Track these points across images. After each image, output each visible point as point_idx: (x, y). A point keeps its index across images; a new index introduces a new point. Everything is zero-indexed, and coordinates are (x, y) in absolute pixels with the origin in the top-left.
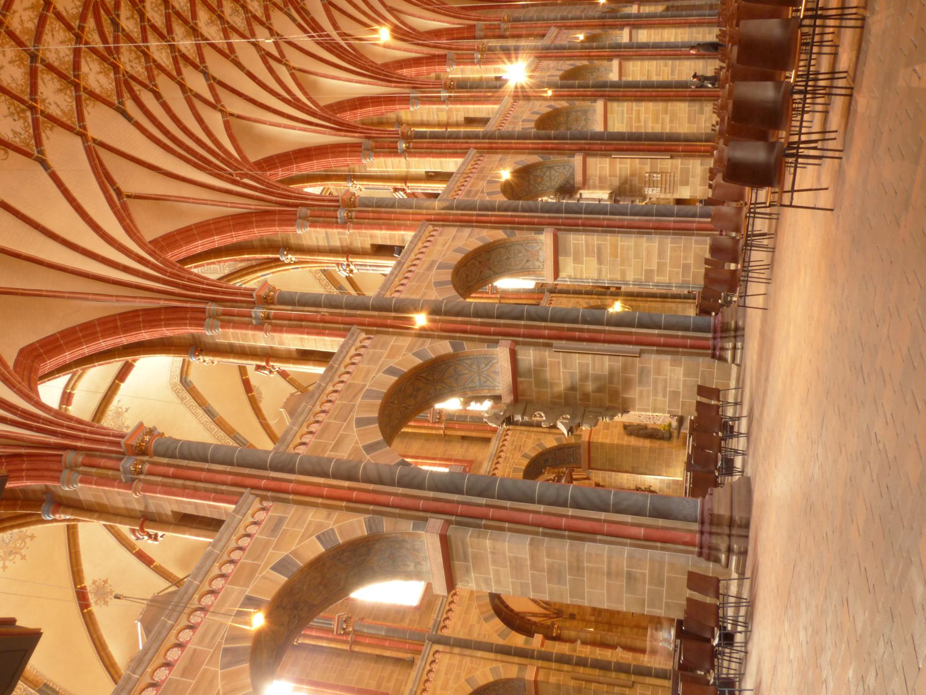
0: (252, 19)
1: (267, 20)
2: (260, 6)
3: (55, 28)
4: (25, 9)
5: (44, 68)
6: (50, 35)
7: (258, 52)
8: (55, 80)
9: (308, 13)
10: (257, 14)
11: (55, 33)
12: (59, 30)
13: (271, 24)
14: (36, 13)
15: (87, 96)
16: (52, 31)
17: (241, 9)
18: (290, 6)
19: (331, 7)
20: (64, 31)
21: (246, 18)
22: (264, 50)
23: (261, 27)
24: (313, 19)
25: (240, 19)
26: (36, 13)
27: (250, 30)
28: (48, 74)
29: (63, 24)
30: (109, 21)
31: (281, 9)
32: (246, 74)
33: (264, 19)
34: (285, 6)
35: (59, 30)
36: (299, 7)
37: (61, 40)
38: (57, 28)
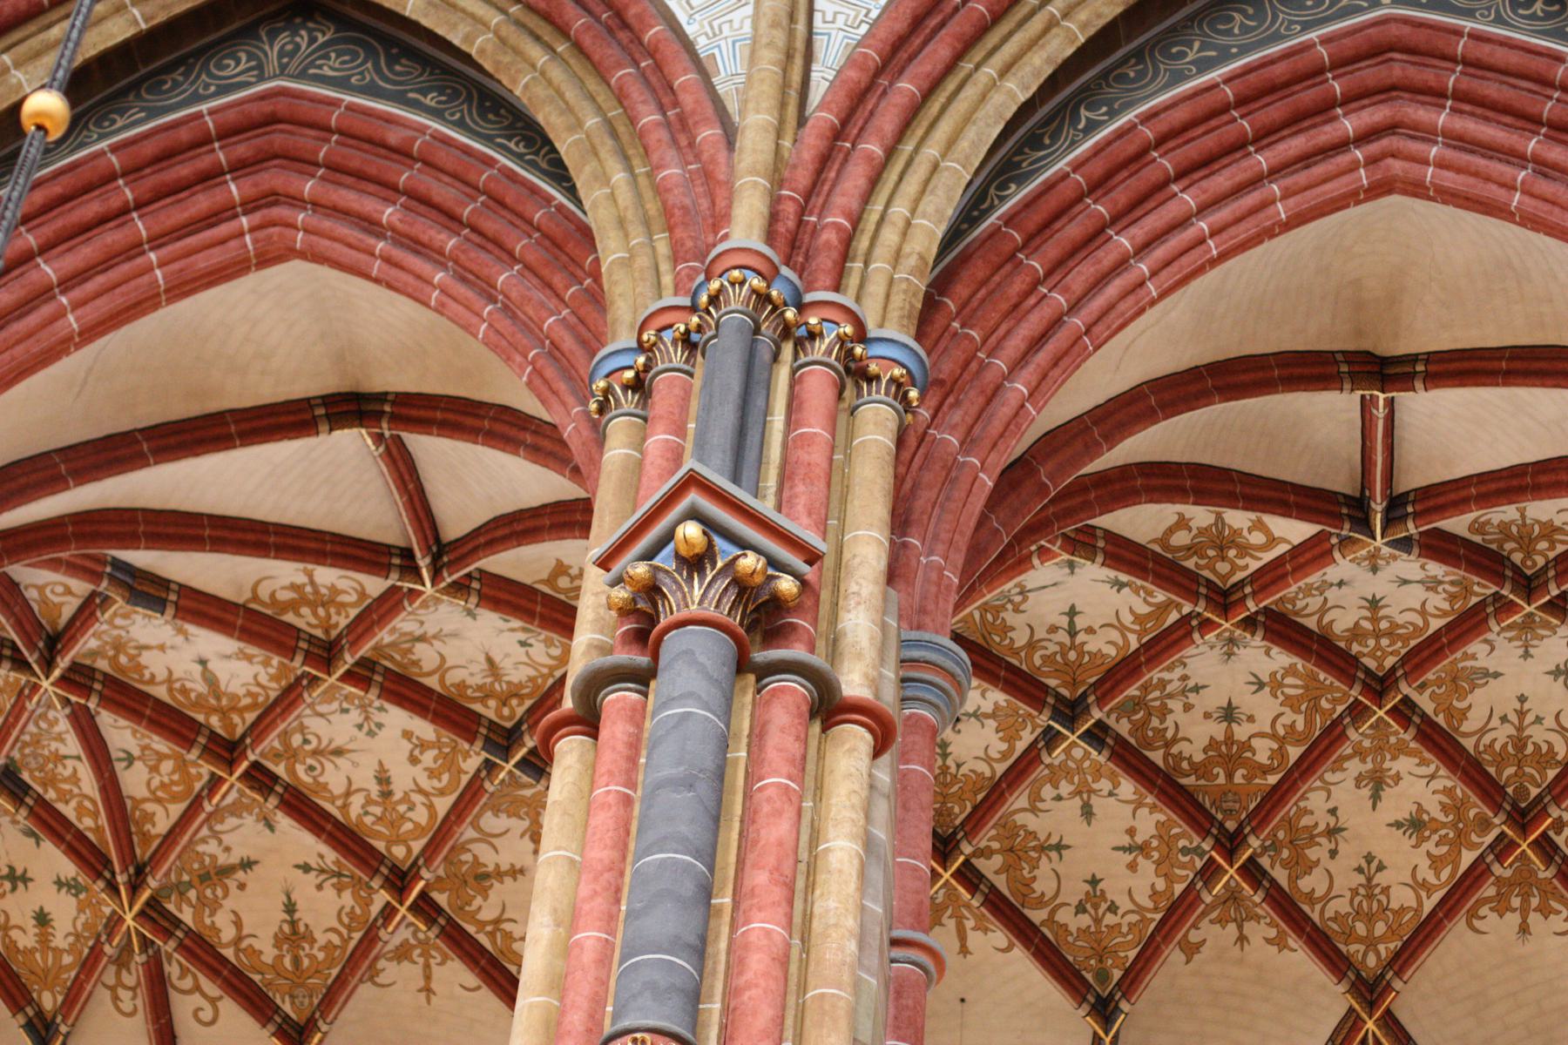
3: (369, 801)
5: (477, 707)
6: (400, 786)
8: (428, 665)
11: (375, 789)
12: (348, 794)
14: (467, 857)
15: (289, 618)
16: (386, 794)
20: (325, 787)
26: (467, 857)
28: (462, 686)
29: (327, 816)
30: (25, 776)
35: (348, 794)
37: (339, 761)
38: (357, 802)
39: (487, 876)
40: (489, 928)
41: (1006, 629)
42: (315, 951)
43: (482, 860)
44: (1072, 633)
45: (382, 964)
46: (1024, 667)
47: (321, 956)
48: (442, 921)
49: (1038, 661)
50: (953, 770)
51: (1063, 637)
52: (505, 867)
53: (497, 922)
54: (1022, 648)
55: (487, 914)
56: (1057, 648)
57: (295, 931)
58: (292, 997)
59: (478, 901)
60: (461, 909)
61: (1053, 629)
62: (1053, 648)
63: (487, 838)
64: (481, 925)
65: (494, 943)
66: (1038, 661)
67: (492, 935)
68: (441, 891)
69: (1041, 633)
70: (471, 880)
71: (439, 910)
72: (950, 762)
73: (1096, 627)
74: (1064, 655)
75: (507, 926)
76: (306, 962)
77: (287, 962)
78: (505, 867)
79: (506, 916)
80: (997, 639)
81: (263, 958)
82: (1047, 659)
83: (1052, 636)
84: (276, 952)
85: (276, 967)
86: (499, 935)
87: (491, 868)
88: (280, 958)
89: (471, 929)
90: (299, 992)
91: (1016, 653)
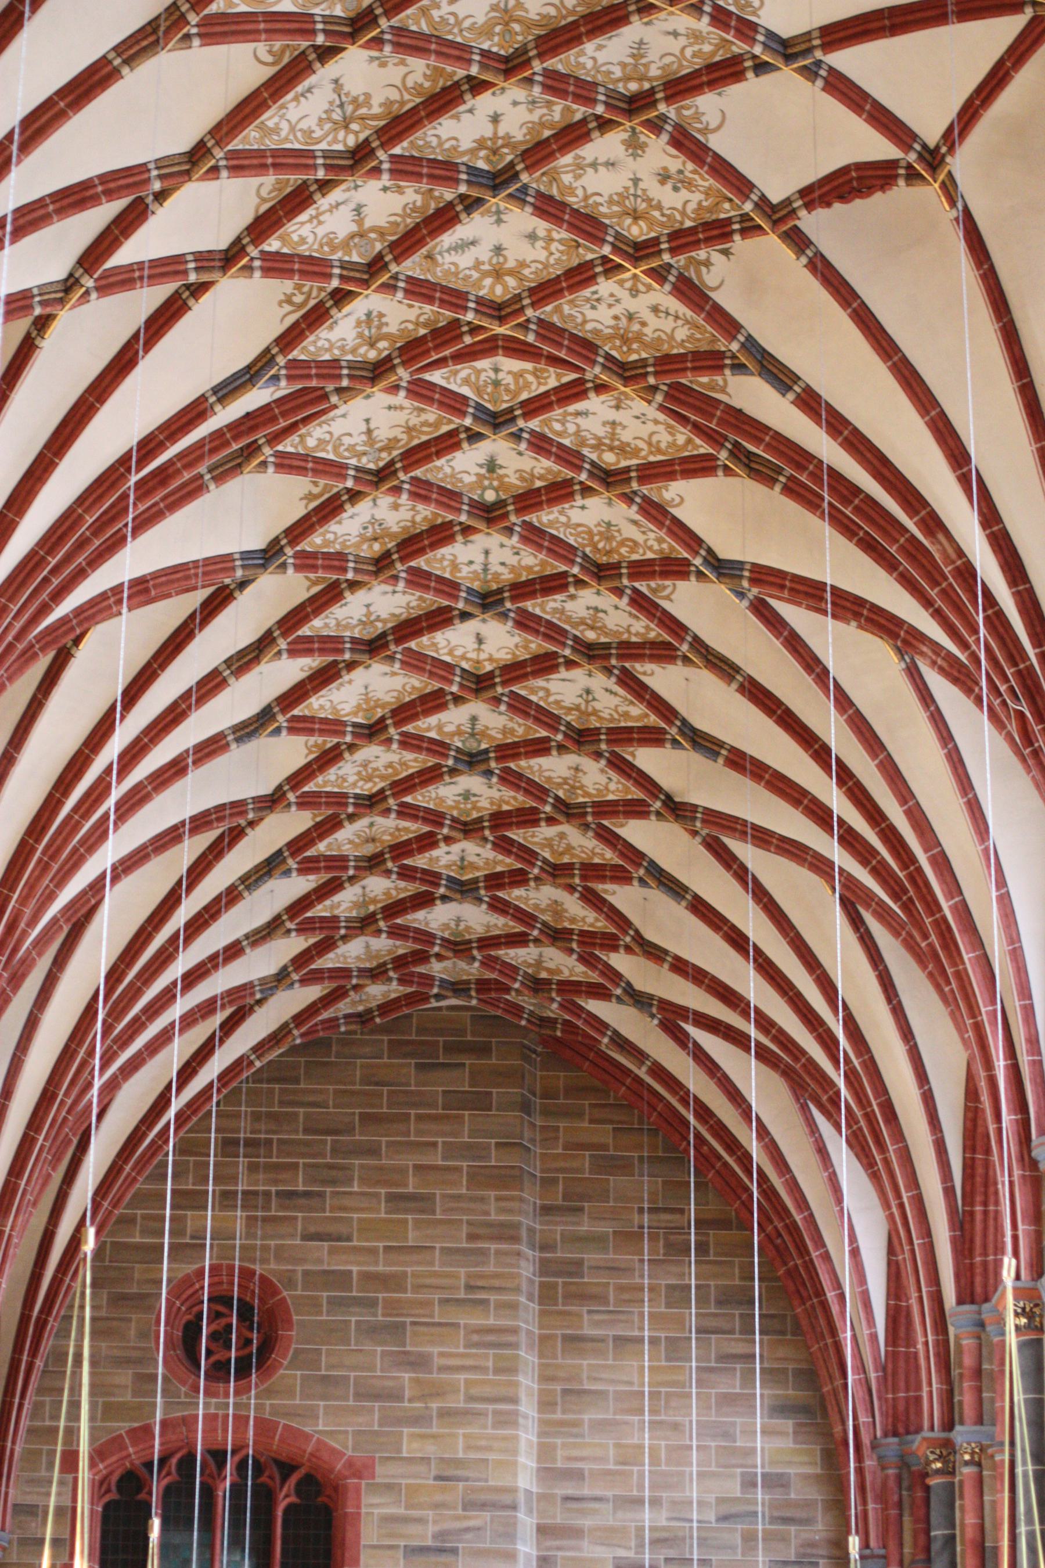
0: (295, 179)
1: (265, 256)
2: (330, 241)
7: (160, 163)
9: (222, 475)
10: (303, 217)
13: (248, 269)
17: (351, 141)
18: (284, 389)
19: (201, 595)
21: (310, 154)
22: (161, 196)
23: (248, 218)
24: (194, 490)
25: (310, 123)
27: (260, 153)
31: (289, 338)
32: (104, 61)
33: (273, 245)
34: (293, 364)
36: (260, 436)
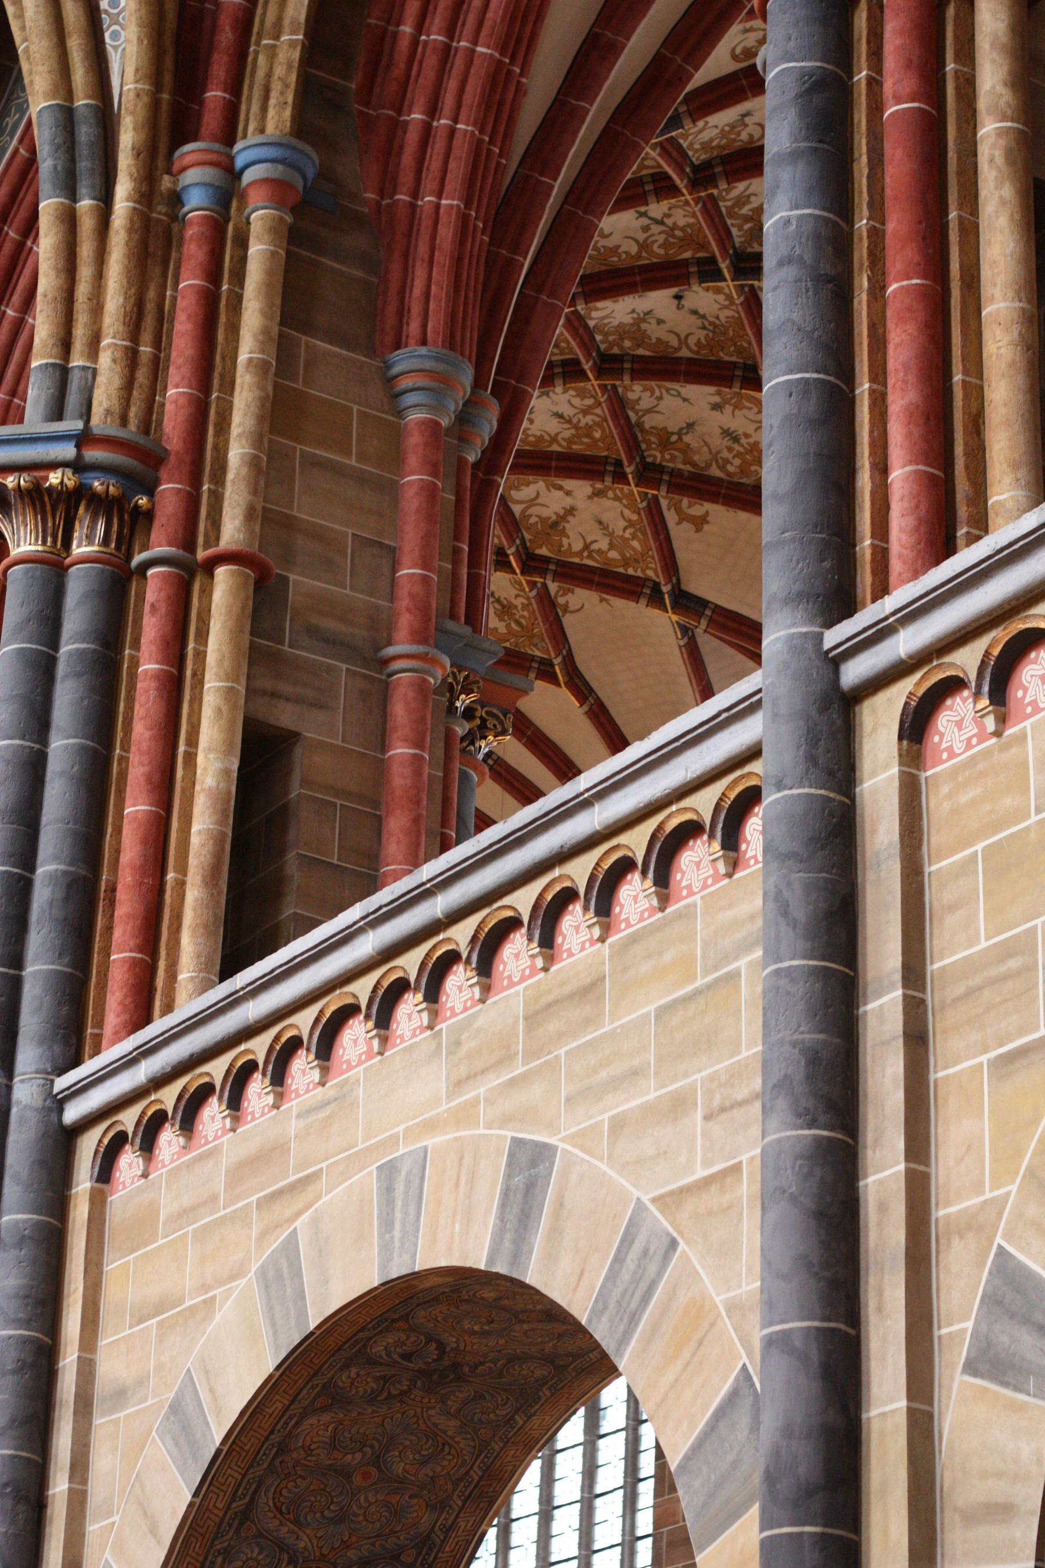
4: (571, 511)
14: (533, 520)
26: (533, 520)
39: (555, 525)
40: (585, 554)
41: (614, 250)
42: (521, 613)
43: (544, 515)
44: (661, 223)
45: (561, 600)
46: (655, 260)
47: (525, 613)
48: (552, 567)
49: (662, 252)
50: (717, 322)
51: (656, 229)
52: (562, 512)
53: (586, 547)
54: (639, 252)
55: (577, 546)
56: (663, 237)
57: (503, 606)
58: (535, 646)
59: (565, 541)
60: (560, 551)
61: (646, 229)
62: (661, 239)
63: (532, 502)
64: (579, 554)
65: (594, 560)
66: (662, 252)
67: (590, 557)
68: (541, 548)
69: (642, 237)
70: (549, 531)
71: (547, 560)
72: (712, 319)
73: (667, 212)
74: (673, 236)
75: (594, 547)
76: (523, 621)
77: (514, 625)
78: (562, 512)
79: (588, 541)
80: (616, 259)
81: (500, 631)
82: (665, 245)
83: (650, 233)
84: (503, 624)
85: (510, 632)
86: (594, 554)
87: (554, 518)
88: (508, 626)
89: (576, 560)
90: (536, 640)
91: (638, 256)
